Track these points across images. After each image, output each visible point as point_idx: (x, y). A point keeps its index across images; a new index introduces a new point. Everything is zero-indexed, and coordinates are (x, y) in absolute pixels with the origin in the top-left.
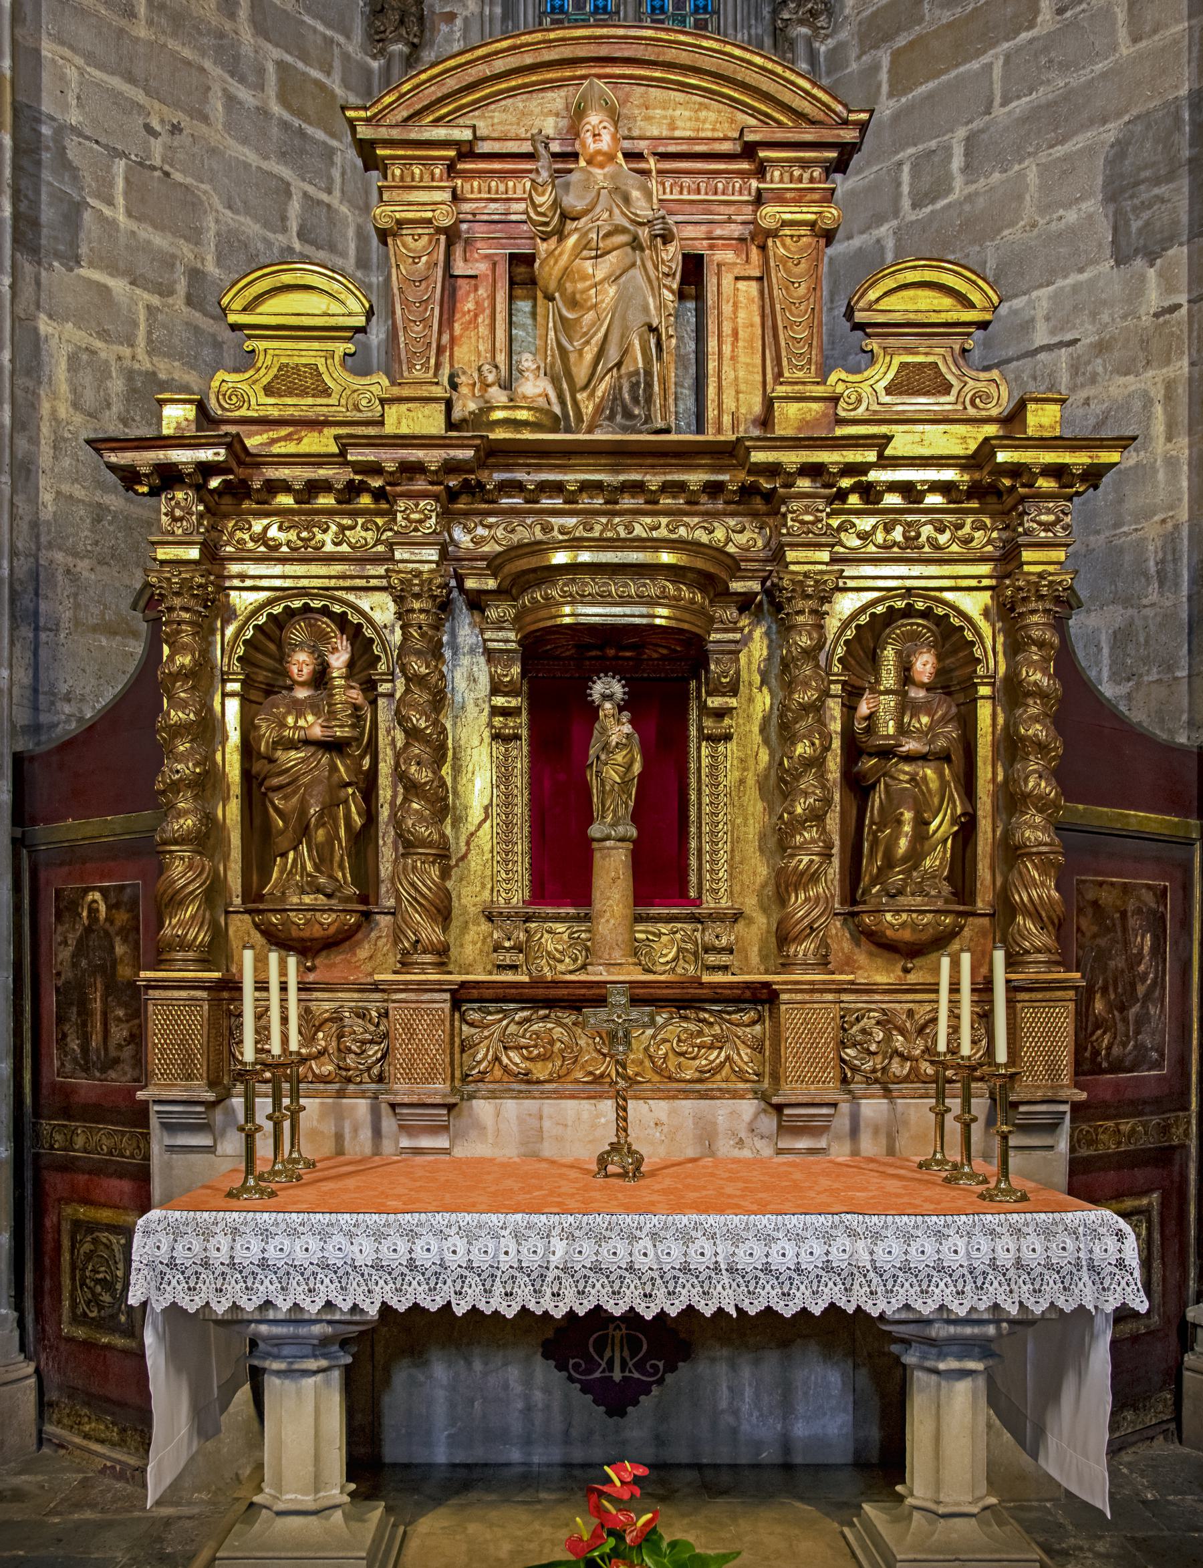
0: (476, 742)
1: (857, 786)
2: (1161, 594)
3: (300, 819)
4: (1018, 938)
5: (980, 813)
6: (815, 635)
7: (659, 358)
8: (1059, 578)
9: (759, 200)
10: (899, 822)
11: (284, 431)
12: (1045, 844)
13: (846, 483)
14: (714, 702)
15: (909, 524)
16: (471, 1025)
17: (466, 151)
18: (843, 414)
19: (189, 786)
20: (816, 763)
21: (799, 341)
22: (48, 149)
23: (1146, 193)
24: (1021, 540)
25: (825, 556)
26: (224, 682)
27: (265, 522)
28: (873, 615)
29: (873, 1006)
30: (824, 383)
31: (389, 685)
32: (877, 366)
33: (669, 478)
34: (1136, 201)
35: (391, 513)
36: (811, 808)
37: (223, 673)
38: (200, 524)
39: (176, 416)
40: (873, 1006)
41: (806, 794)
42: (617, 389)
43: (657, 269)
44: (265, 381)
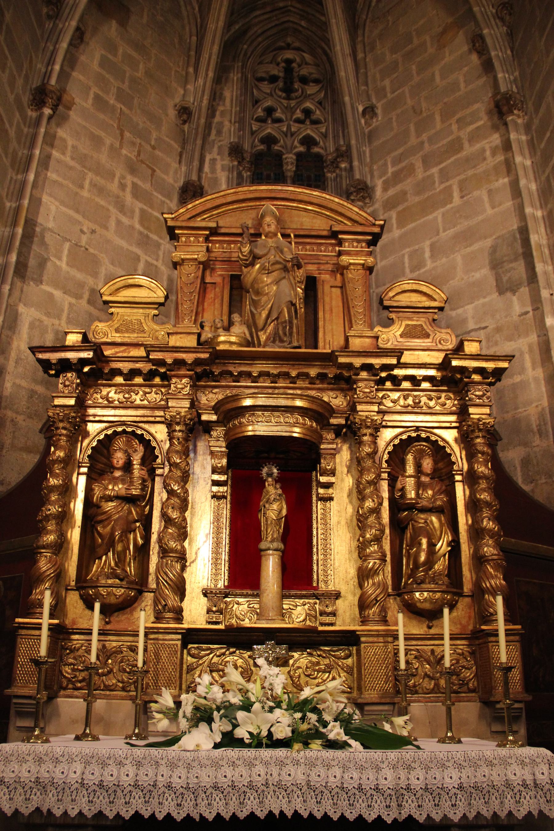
0: (204, 500)
1: (398, 526)
2: (541, 440)
3: (110, 538)
4: (487, 607)
5: (461, 541)
6: (372, 446)
7: (296, 318)
8: (487, 421)
9: (340, 254)
10: (420, 544)
11: (122, 348)
12: (495, 555)
13: (383, 374)
14: (323, 479)
15: (415, 396)
16: (193, 656)
17: (214, 232)
18: (381, 346)
19: (54, 518)
20: (376, 511)
21: (359, 313)
22: (37, 236)
23: (507, 266)
24: (468, 403)
25: (375, 408)
26: (79, 467)
27: (109, 389)
28: (401, 440)
29: (412, 648)
30: (372, 329)
31: (161, 470)
32: (396, 325)
33: (301, 371)
34: (504, 269)
35: (169, 386)
36: (375, 536)
37: (79, 463)
38: (77, 389)
39: (73, 339)
40: (412, 648)
41: (371, 527)
42: (276, 329)
43: (295, 279)
44: (116, 326)
